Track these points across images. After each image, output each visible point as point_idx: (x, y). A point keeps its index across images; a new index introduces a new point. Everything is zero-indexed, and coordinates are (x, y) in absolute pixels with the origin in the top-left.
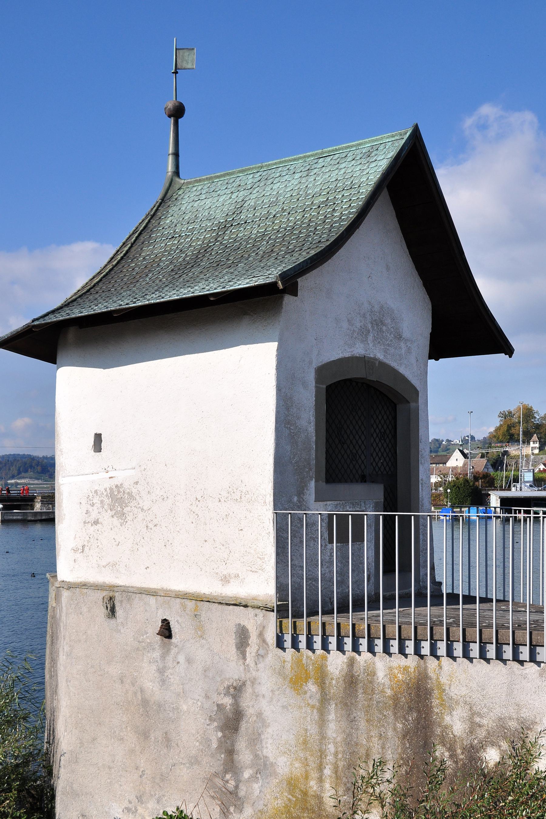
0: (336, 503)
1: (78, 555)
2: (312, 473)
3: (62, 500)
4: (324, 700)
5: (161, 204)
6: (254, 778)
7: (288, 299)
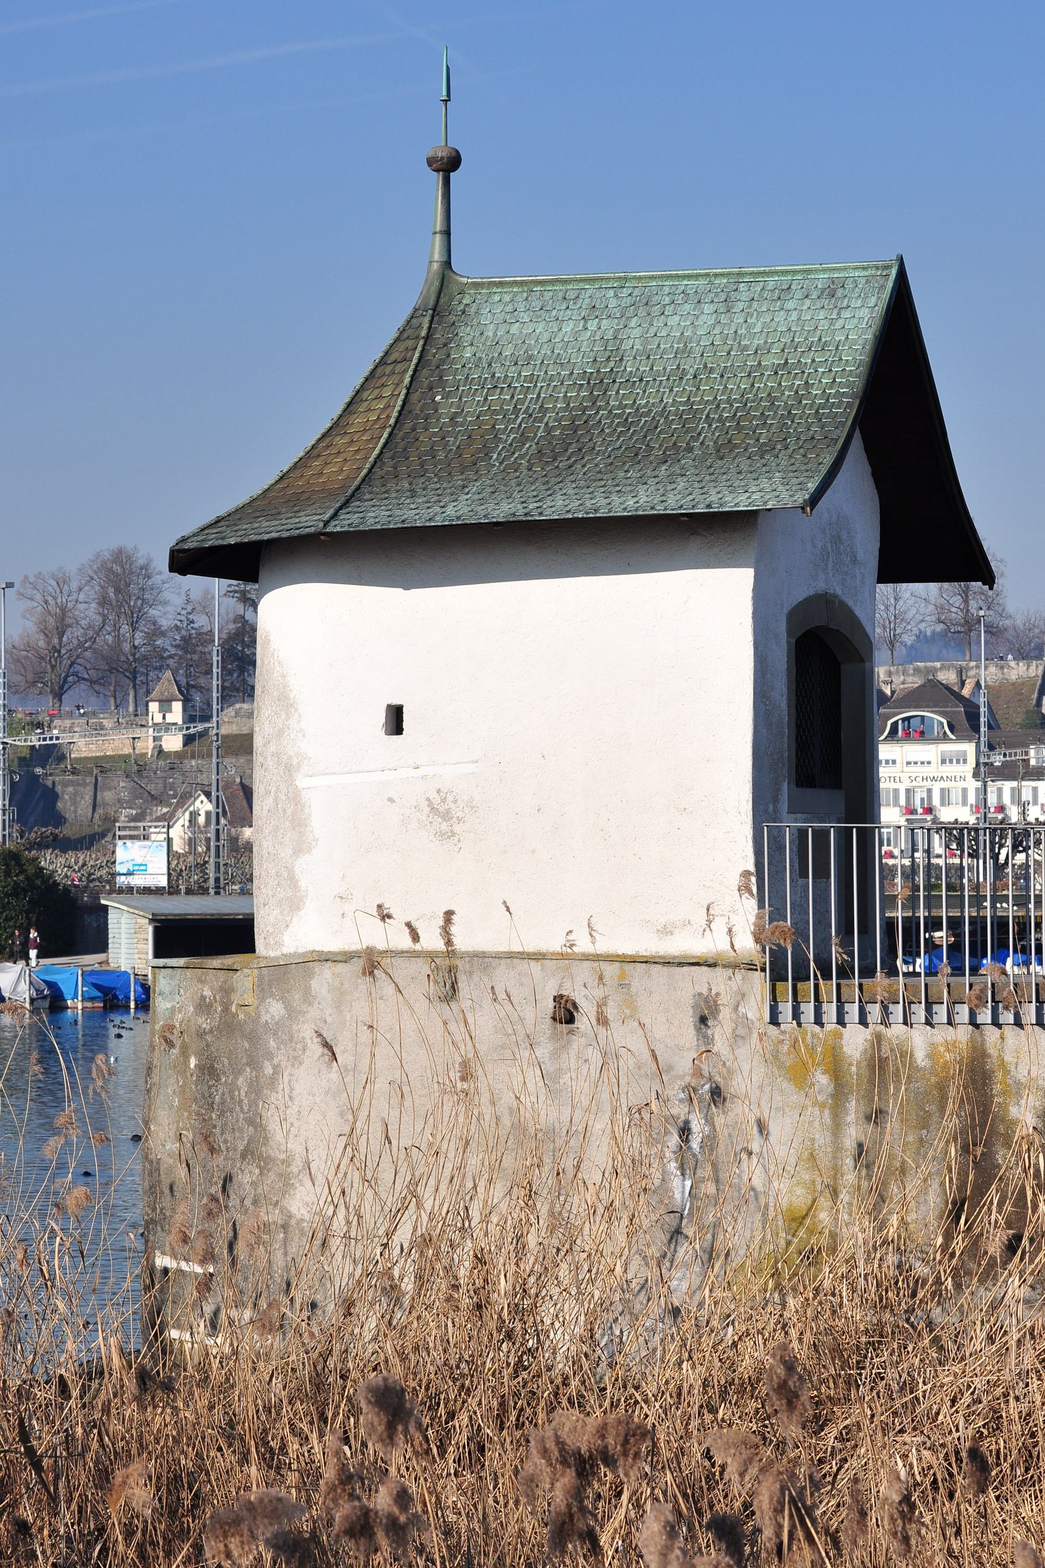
2: (785, 771)
3: (310, 815)
5: (433, 317)
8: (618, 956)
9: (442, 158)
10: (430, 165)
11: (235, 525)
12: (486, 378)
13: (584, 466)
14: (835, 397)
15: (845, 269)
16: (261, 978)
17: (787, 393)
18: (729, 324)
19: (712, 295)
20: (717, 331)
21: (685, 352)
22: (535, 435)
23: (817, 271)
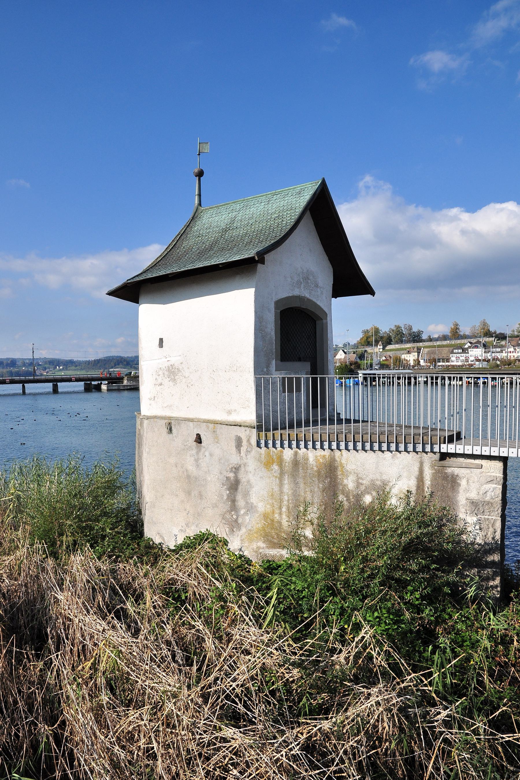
0: (286, 372)
1: (152, 402)
2: (274, 356)
4: (282, 473)
6: (246, 514)
7: (260, 266)
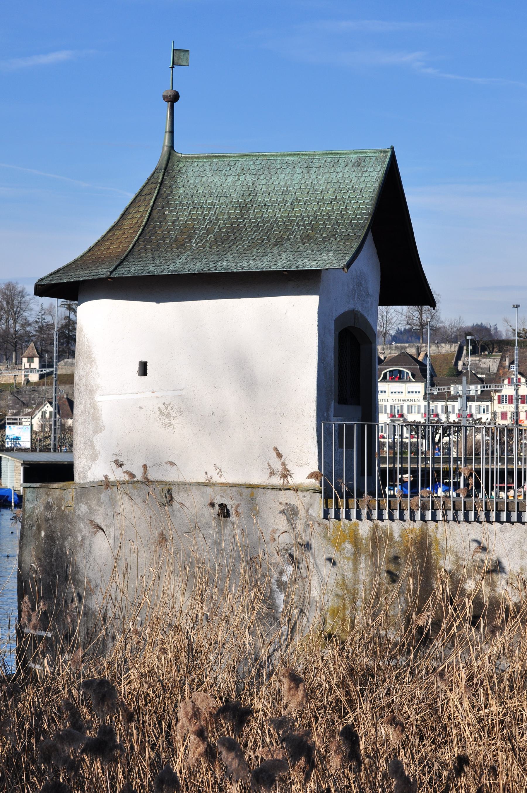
3: (101, 414)
8: (250, 485)
9: (170, 96)
10: (164, 99)
11: (67, 273)
12: (190, 203)
13: (237, 247)
14: (359, 215)
15: (365, 152)
16: (76, 493)
17: (336, 213)
18: (309, 179)
19: (300, 164)
20: (302, 182)
21: (287, 192)
22: (214, 231)
23: (352, 153)
